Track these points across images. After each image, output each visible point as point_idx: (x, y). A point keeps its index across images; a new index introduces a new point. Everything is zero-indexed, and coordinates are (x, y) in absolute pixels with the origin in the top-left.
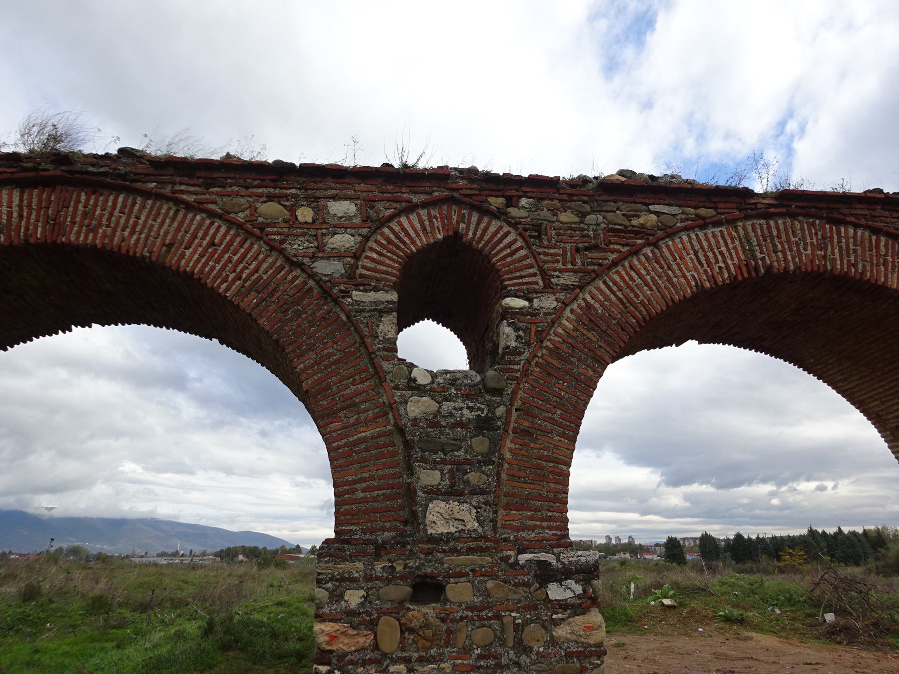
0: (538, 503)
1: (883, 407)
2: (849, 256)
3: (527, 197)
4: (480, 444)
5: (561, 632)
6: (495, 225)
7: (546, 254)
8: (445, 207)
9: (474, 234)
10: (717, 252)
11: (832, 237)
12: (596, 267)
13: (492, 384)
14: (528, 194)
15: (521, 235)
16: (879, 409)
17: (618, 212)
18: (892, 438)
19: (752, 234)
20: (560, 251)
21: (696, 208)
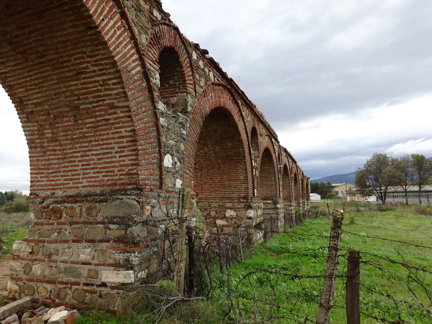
1: (26, 94)
16: (23, 95)
18: (26, 120)
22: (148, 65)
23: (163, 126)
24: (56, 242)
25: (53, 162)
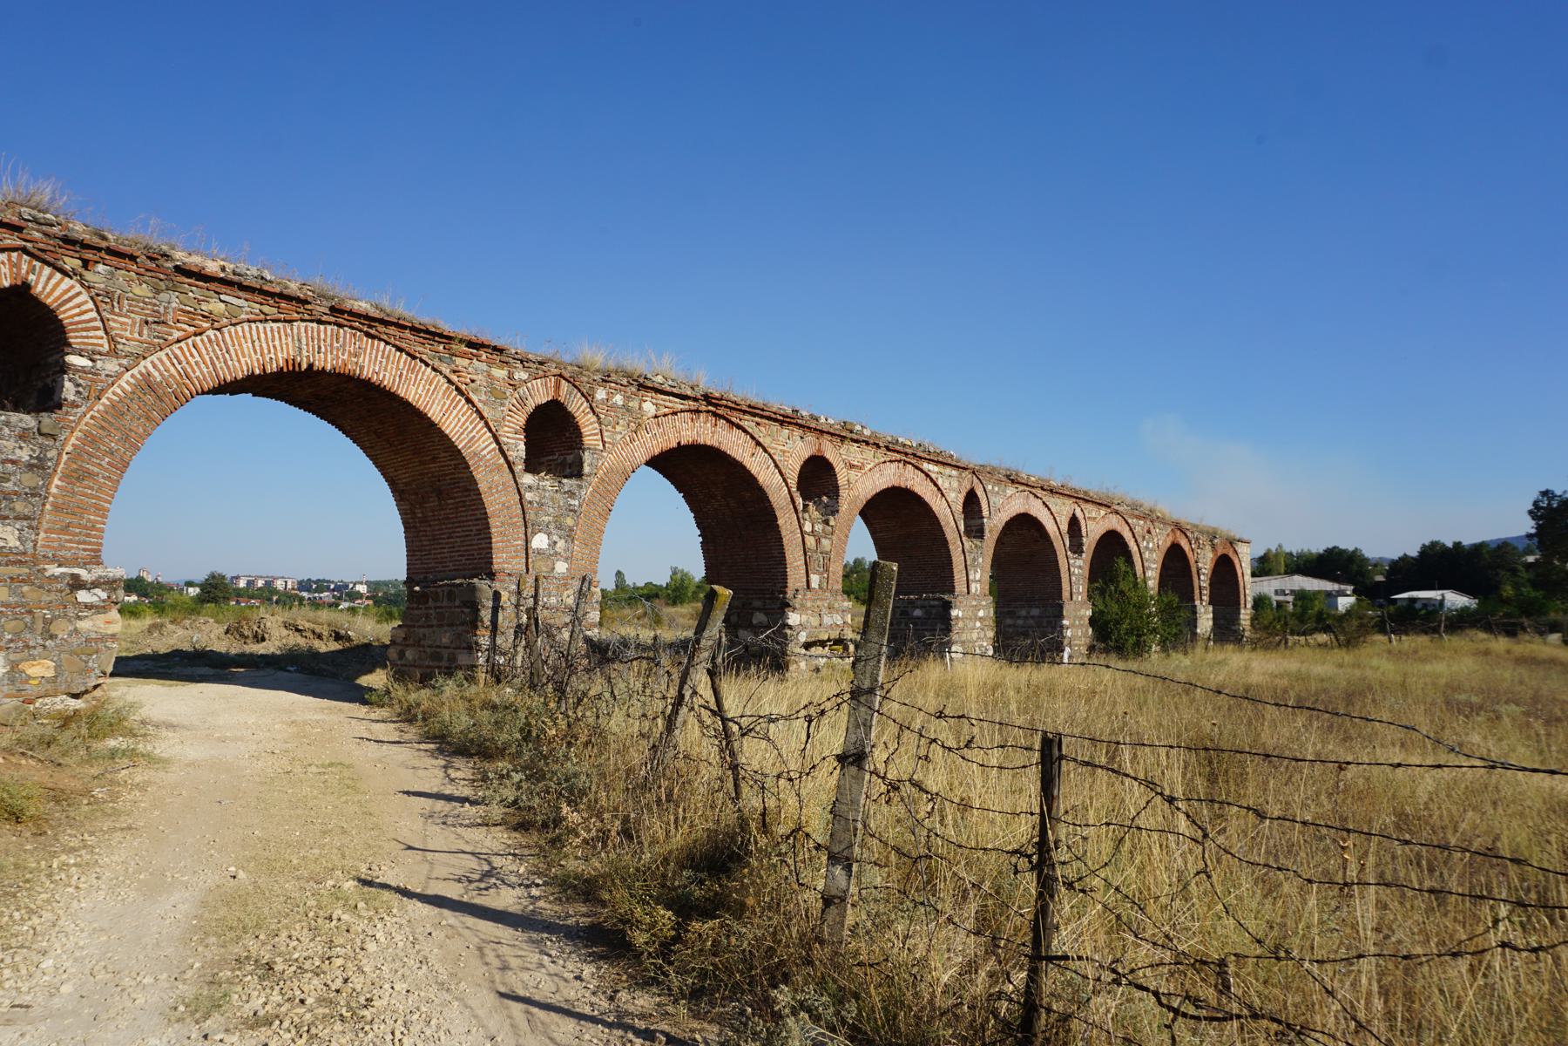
0: (78, 531)
2: (375, 364)
3: (104, 264)
4: (30, 480)
5: (83, 625)
6: (67, 282)
7: (114, 321)
8: (15, 255)
9: (44, 288)
10: (271, 344)
11: (366, 348)
12: (161, 341)
13: (45, 430)
14: (106, 262)
15: (92, 298)
17: (191, 294)
19: (303, 334)
20: (129, 321)
21: (261, 304)
22: (505, 439)
23: (530, 502)
24: (423, 627)
25: (425, 543)
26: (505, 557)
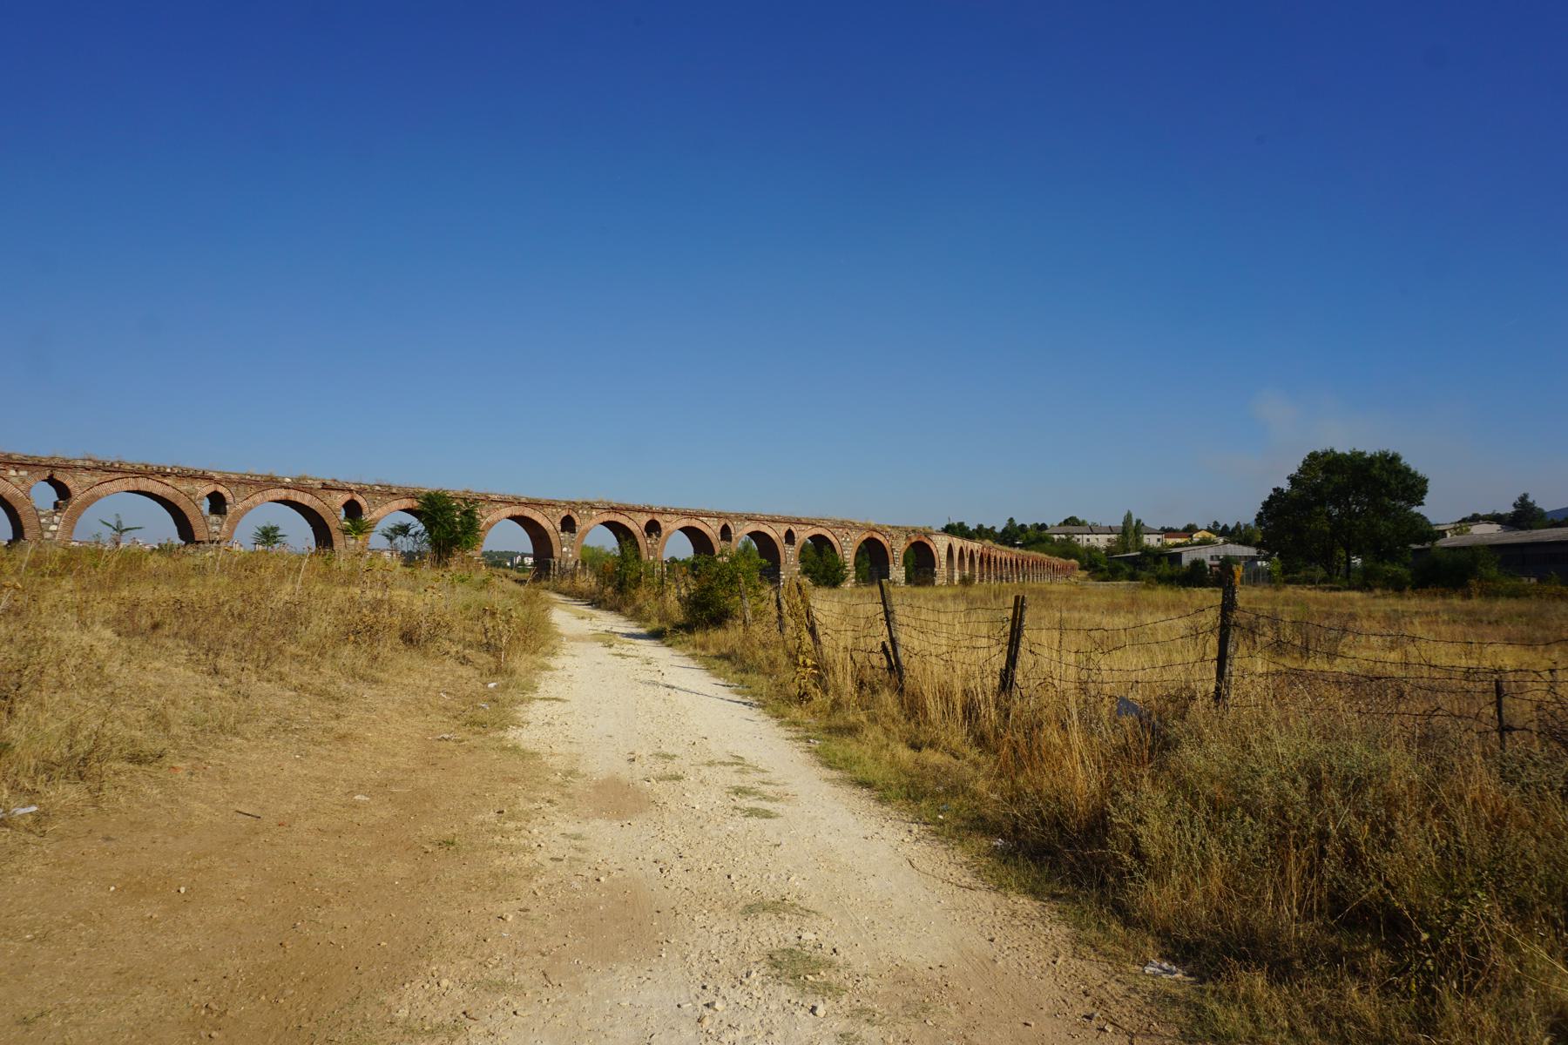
26: (556, 553)
